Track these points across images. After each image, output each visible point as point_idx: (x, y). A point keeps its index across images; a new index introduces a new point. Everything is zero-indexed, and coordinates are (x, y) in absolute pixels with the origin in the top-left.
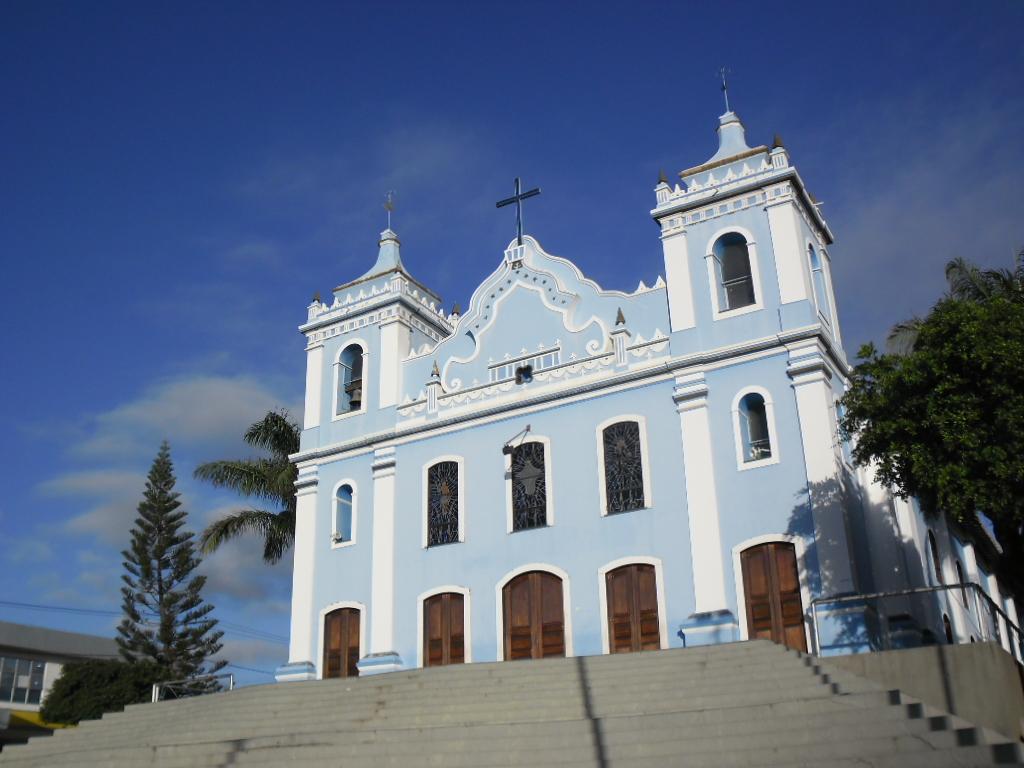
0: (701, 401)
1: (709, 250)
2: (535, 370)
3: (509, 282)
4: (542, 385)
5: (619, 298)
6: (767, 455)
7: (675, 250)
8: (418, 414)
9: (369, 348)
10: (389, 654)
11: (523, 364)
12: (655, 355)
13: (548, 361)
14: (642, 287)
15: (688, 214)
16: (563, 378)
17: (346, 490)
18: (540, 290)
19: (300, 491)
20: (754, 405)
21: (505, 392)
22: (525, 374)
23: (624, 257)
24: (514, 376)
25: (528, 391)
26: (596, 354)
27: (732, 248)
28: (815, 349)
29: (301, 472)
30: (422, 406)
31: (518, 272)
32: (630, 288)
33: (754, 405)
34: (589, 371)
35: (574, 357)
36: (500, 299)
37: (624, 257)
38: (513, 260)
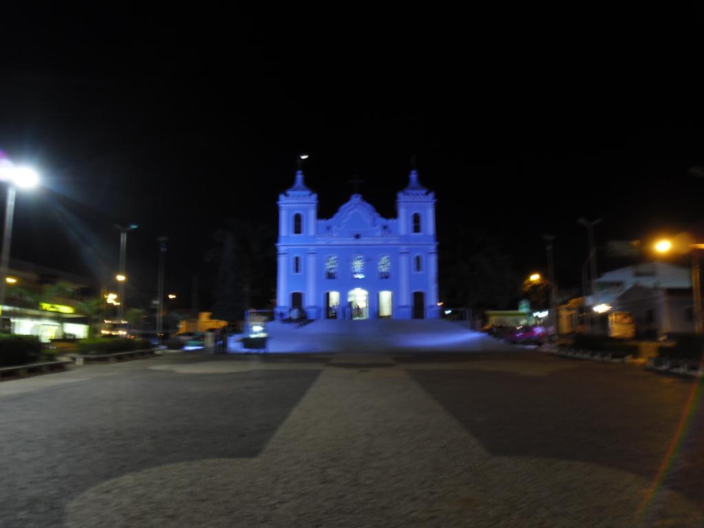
5: (383, 221)
7: (402, 212)
8: (324, 240)
14: (390, 221)
17: (297, 259)
20: (418, 259)
22: (358, 237)
23: (387, 210)
27: (417, 219)
33: (418, 259)
36: (352, 212)
37: (387, 210)
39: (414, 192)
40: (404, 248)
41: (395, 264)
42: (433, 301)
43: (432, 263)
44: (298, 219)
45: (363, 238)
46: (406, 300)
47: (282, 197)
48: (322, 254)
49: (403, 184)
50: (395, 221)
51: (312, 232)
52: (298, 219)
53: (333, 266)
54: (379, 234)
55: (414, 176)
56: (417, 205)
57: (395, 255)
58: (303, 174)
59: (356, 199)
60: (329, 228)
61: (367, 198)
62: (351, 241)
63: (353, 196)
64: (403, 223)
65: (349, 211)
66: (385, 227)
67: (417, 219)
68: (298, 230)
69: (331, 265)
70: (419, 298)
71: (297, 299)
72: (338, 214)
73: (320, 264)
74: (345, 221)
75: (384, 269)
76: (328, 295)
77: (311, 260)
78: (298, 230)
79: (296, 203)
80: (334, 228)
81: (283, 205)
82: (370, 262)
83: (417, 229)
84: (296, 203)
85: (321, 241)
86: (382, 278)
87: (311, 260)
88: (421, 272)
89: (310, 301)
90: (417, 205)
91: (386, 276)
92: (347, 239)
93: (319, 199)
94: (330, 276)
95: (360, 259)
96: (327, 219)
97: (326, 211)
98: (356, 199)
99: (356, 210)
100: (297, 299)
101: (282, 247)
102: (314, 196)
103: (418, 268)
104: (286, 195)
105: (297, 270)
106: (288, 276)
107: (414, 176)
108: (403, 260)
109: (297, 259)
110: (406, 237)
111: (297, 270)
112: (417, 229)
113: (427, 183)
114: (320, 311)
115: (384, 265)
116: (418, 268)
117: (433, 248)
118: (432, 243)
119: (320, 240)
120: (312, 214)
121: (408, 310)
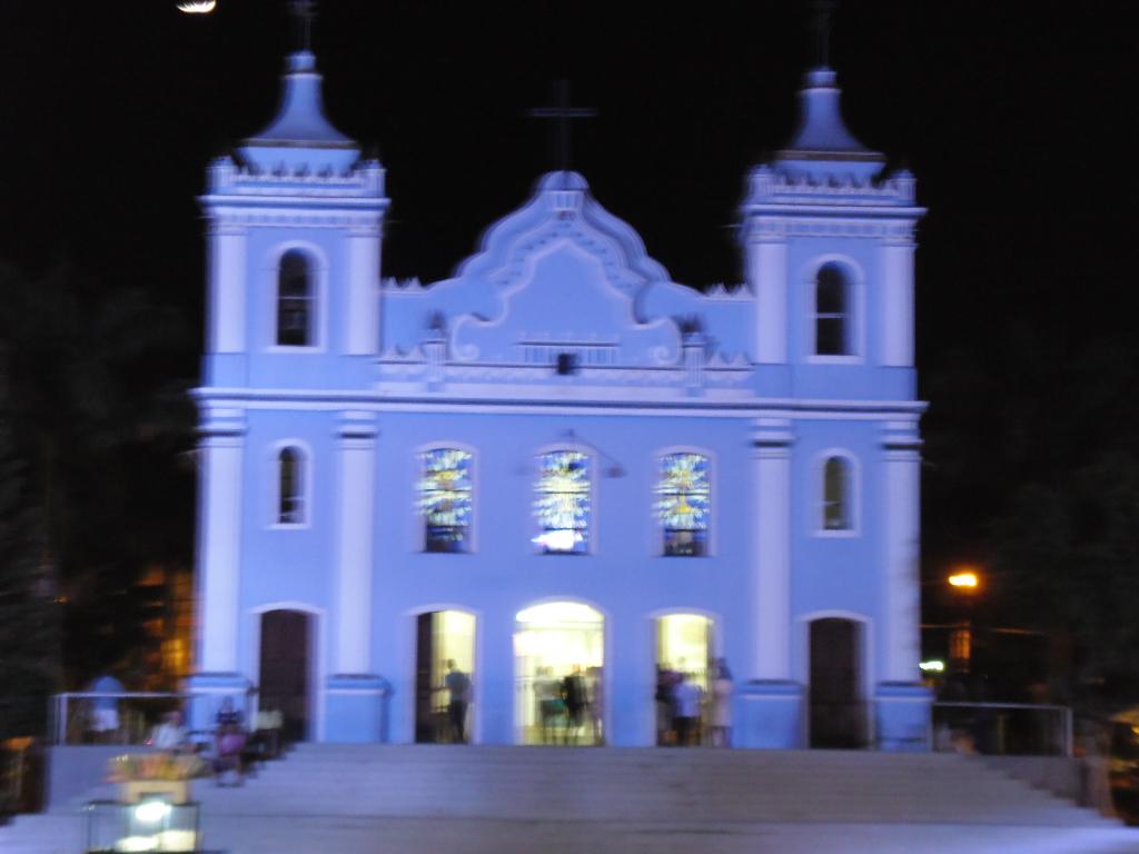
3: (555, 235)
5: (685, 299)
8: (411, 378)
10: (366, 677)
11: (567, 350)
12: (736, 385)
14: (718, 296)
19: (214, 441)
20: (835, 469)
21: (538, 382)
22: (565, 365)
23: (702, 250)
25: (567, 389)
28: (914, 426)
29: (215, 413)
33: (835, 469)
34: (653, 384)
37: (702, 250)
39: (819, 168)
40: (771, 423)
41: (733, 496)
42: (895, 658)
43: (893, 495)
44: (295, 276)
45: (587, 374)
46: (778, 655)
47: (224, 172)
48: (398, 438)
49: (774, 132)
50: (741, 295)
51: (359, 339)
52: (295, 276)
53: (450, 496)
54: (660, 354)
55: (821, 94)
56: (836, 228)
57: (732, 447)
58: (318, 67)
59: (560, 194)
60: (437, 322)
61: (609, 193)
62: (541, 384)
63: (553, 179)
64: (769, 307)
65: (530, 247)
66: (688, 327)
67: (831, 289)
68: (294, 327)
69: (444, 488)
70: (833, 645)
71: (286, 642)
72: (473, 264)
73: (390, 488)
74: (506, 294)
75: (684, 517)
76: (425, 624)
77: (355, 464)
78: (294, 327)
79: (288, 202)
80: (457, 323)
81: (220, 211)
82: (615, 478)
83: (831, 338)
84: (288, 202)
85: (398, 383)
86: (670, 552)
87: (355, 464)
89: (347, 645)
90: (836, 228)
91: (684, 546)
92: (518, 373)
93: (390, 187)
94: (438, 540)
95: (573, 467)
96: (426, 281)
97: (423, 245)
98: (560, 194)
99: (562, 243)
100: (286, 642)
101: (222, 400)
102: (375, 174)
103: (835, 512)
104: (240, 163)
105: (288, 507)
106: (248, 538)
107: (821, 94)
108: (770, 471)
109: (288, 458)
110: (787, 368)
111: (288, 507)
112: (831, 338)
113: (877, 128)
114: (388, 691)
115: (681, 493)
116: (835, 512)
117: (903, 427)
119: (391, 378)
120: (363, 252)
121: (790, 704)
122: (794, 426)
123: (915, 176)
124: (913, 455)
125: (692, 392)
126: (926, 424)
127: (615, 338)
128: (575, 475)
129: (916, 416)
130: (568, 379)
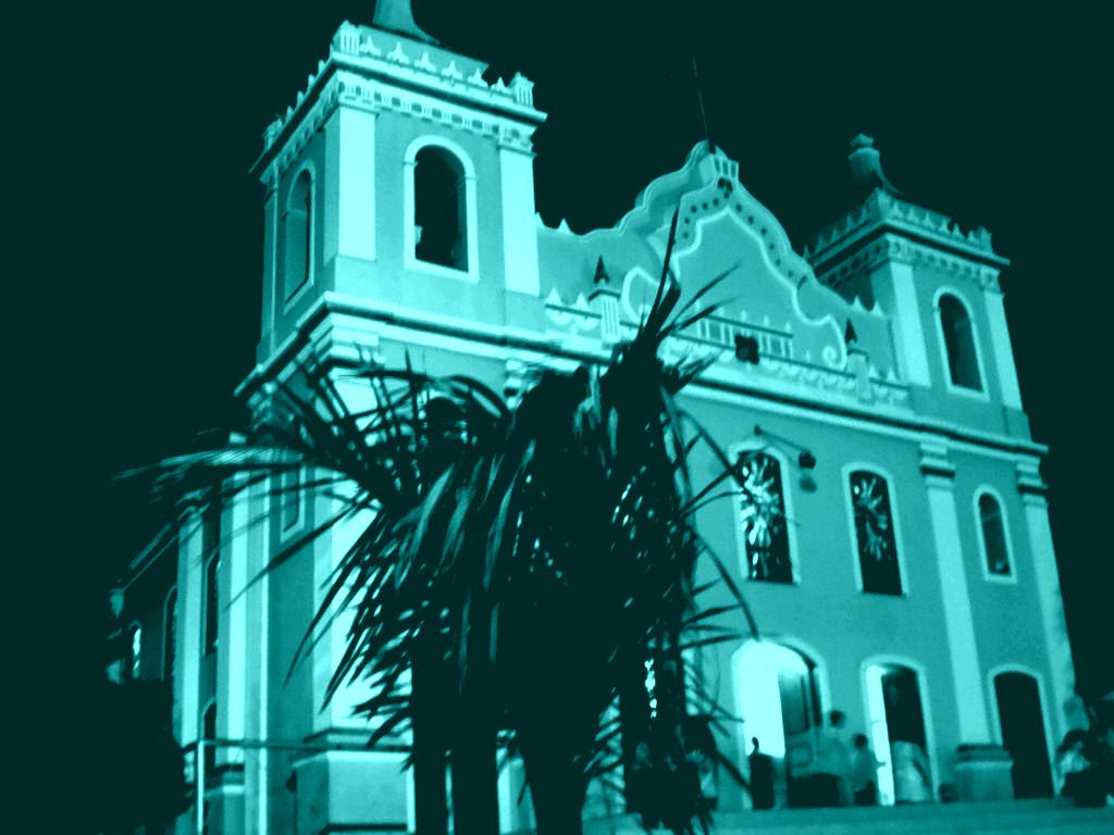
0: (946, 482)
1: (936, 302)
2: (761, 349)
4: (771, 375)
6: (1006, 571)
9: (477, 171)
13: (776, 346)
15: (915, 247)
16: (795, 379)
18: (761, 242)
22: (747, 350)
24: (732, 343)
26: (831, 365)
30: (591, 323)
31: (726, 196)
32: (850, 300)
35: (808, 357)
38: (722, 174)
44: (438, 181)
52: (438, 181)
59: (712, 165)
68: (442, 240)
78: (442, 240)
88: (1013, 579)
96: (579, 228)
98: (712, 165)
99: (727, 211)
107: (868, 152)
108: (941, 501)
117: (1029, 466)
118: (1028, 443)
119: (563, 329)
120: (518, 174)
122: (951, 455)
123: (989, 230)
124: (1041, 500)
125: (862, 401)
126: (1044, 471)
127: (788, 328)
128: (766, 485)
129: (1036, 461)
130: (749, 366)
